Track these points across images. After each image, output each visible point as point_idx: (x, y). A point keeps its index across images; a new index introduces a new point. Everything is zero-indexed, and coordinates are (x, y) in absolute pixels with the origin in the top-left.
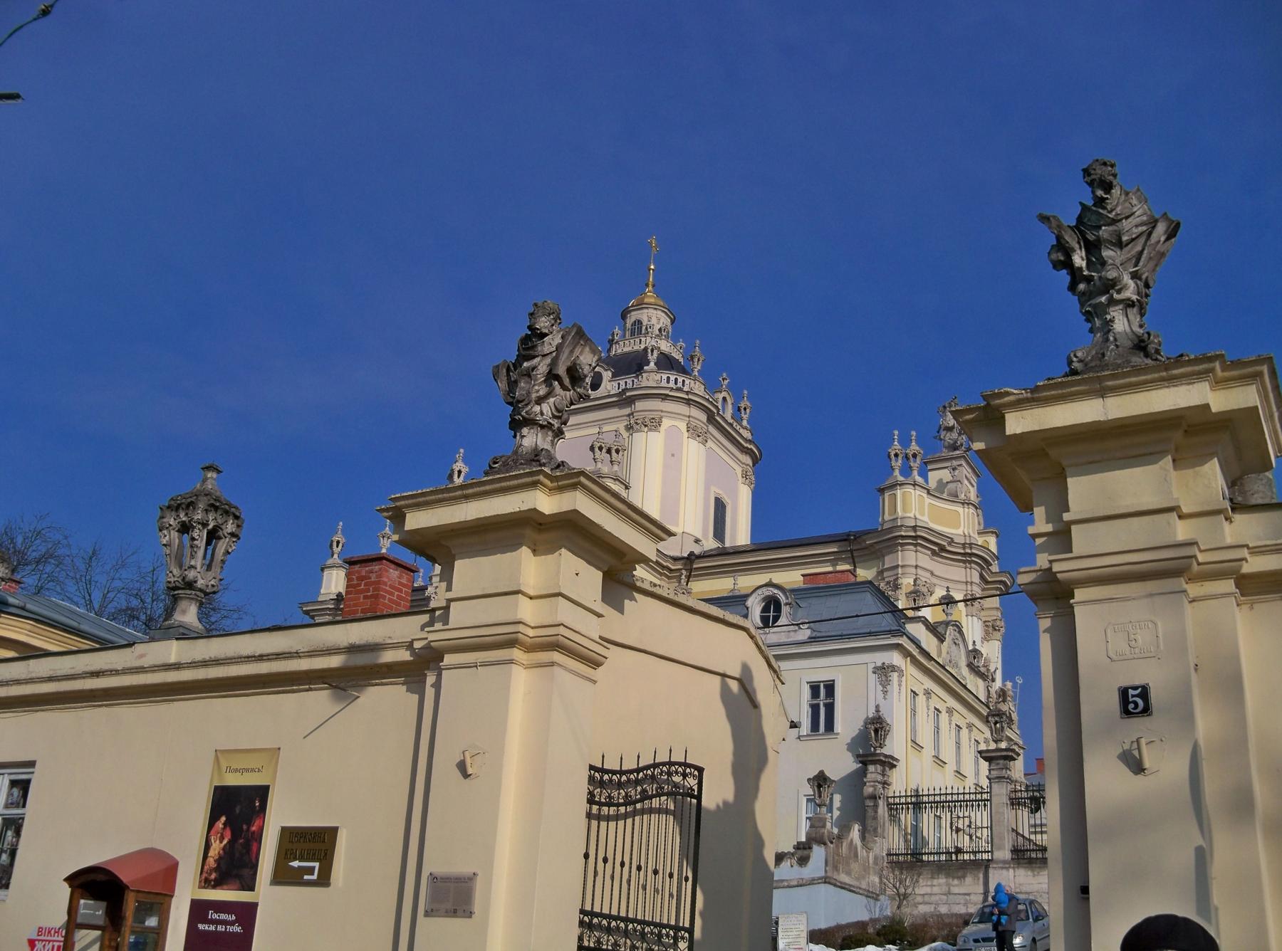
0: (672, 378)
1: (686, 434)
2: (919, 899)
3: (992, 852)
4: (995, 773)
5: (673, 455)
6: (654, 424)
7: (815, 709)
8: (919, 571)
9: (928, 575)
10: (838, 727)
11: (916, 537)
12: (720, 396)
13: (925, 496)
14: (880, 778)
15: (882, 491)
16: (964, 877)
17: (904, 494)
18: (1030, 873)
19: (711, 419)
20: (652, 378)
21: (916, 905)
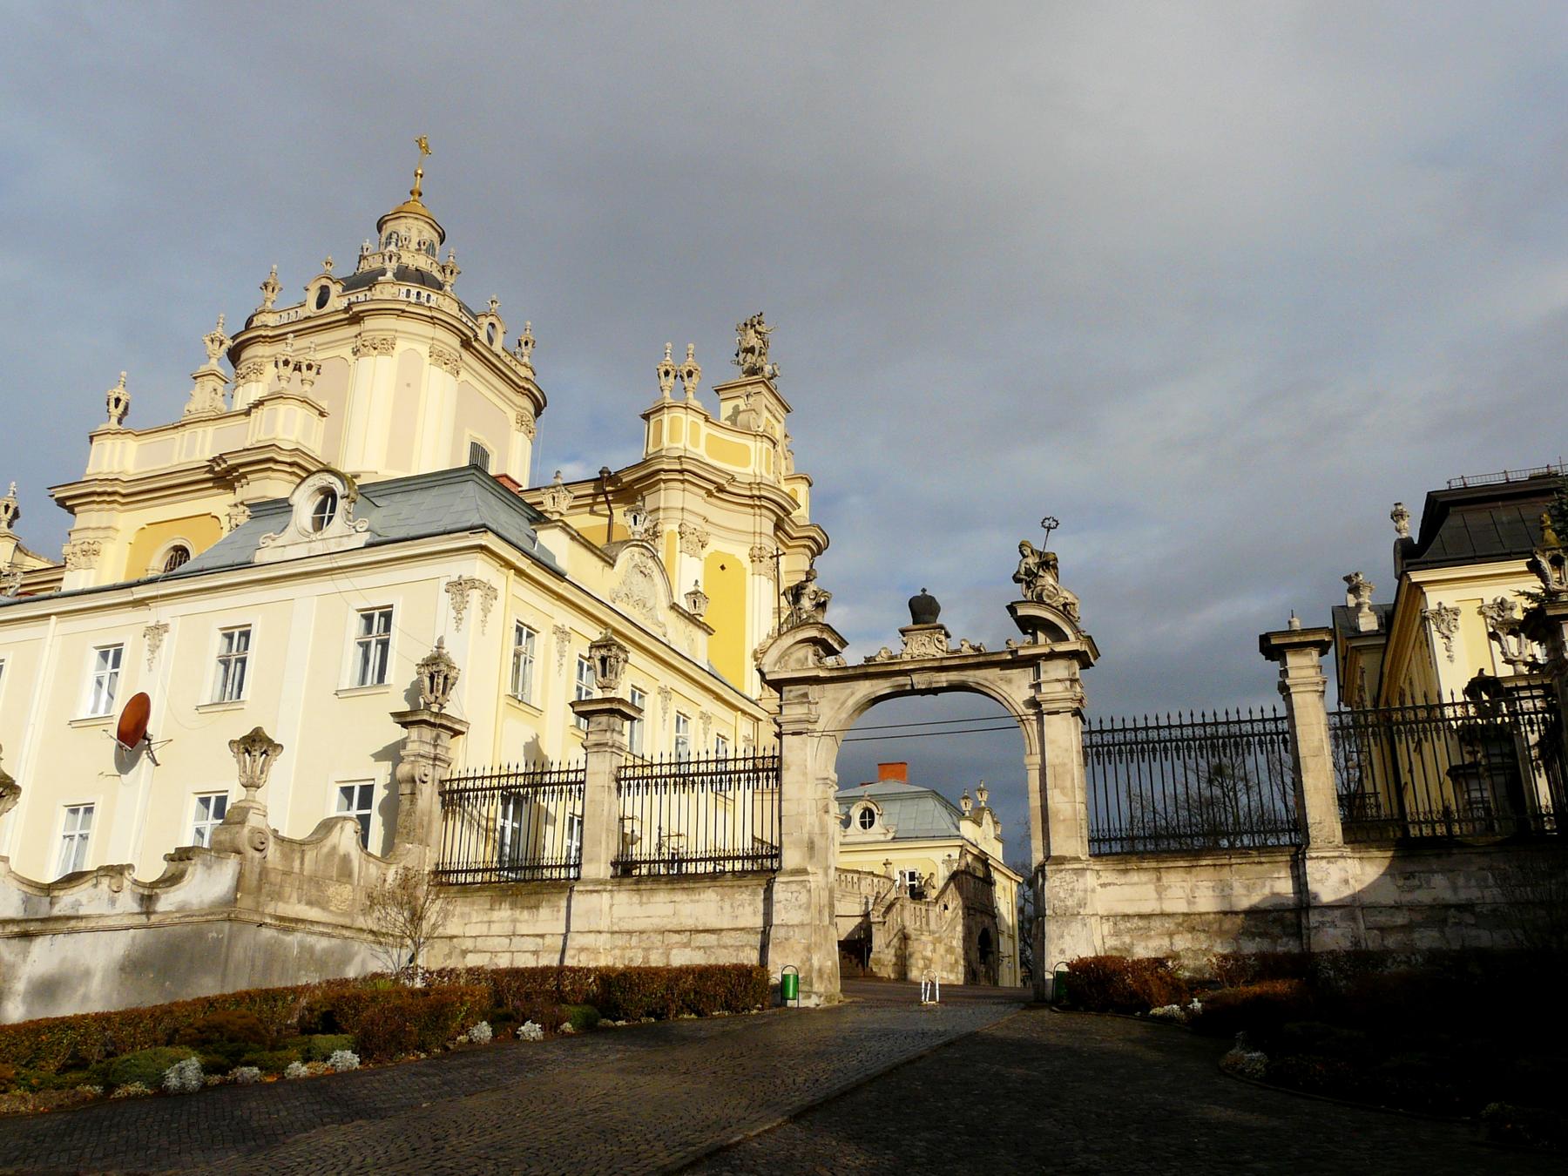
0: (414, 291)
1: (428, 360)
2: (469, 944)
3: (578, 866)
4: (593, 738)
5: (408, 385)
6: (384, 346)
7: (366, 646)
8: (686, 515)
9: (700, 521)
10: (389, 678)
11: (681, 472)
12: (485, 322)
13: (700, 421)
14: (428, 749)
15: (646, 417)
16: (537, 907)
17: (672, 420)
18: (635, 898)
19: (466, 344)
20: (387, 291)
21: (464, 953)
